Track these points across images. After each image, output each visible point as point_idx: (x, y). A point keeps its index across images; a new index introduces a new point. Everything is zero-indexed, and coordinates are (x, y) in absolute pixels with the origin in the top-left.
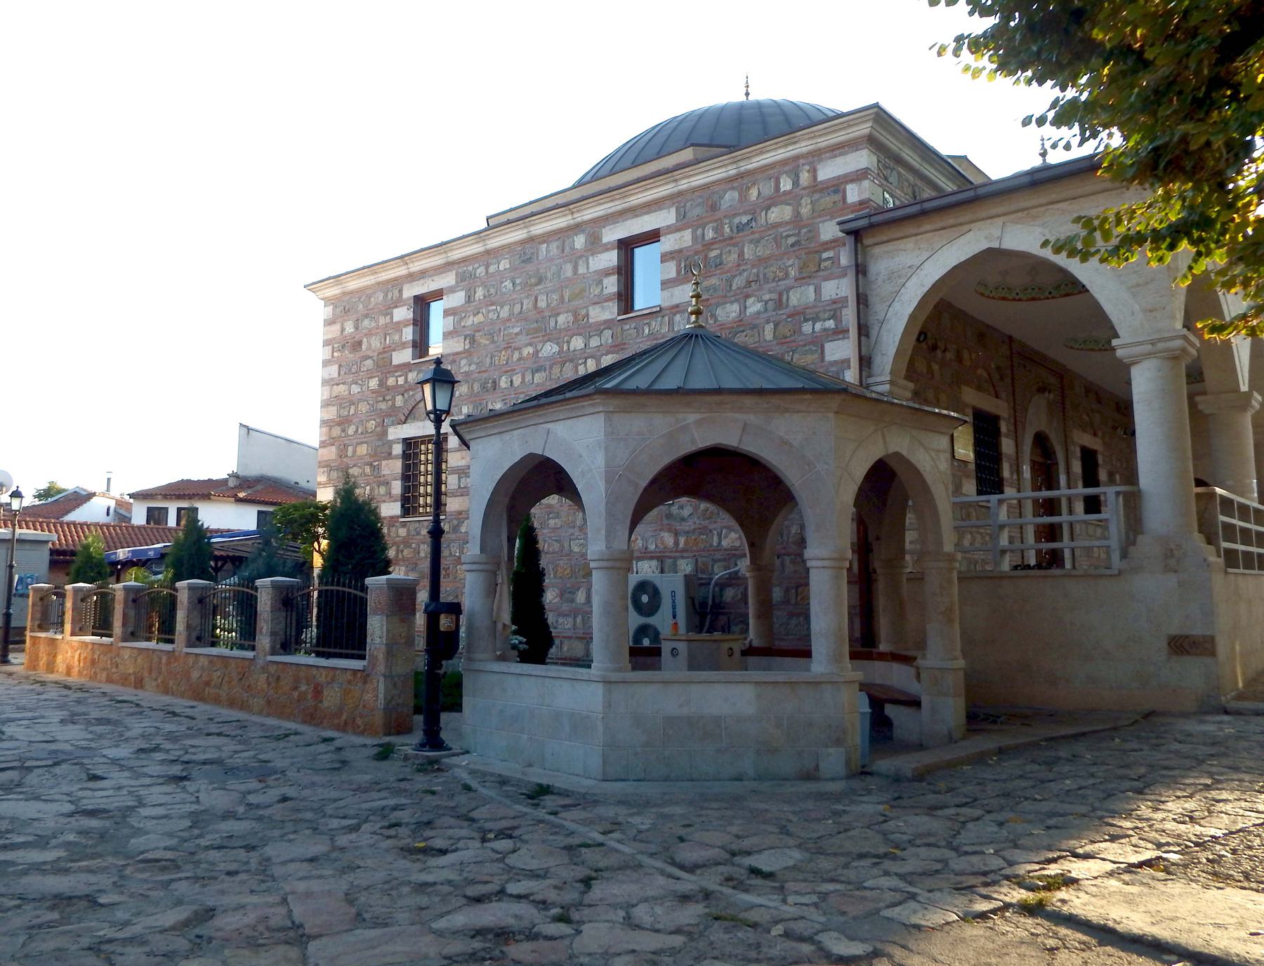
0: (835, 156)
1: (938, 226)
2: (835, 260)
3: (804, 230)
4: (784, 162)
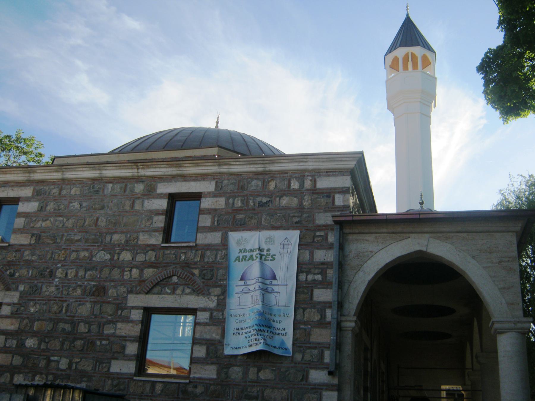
0: (329, 176)
2: (326, 238)
3: (305, 215)
4: (294, 172)
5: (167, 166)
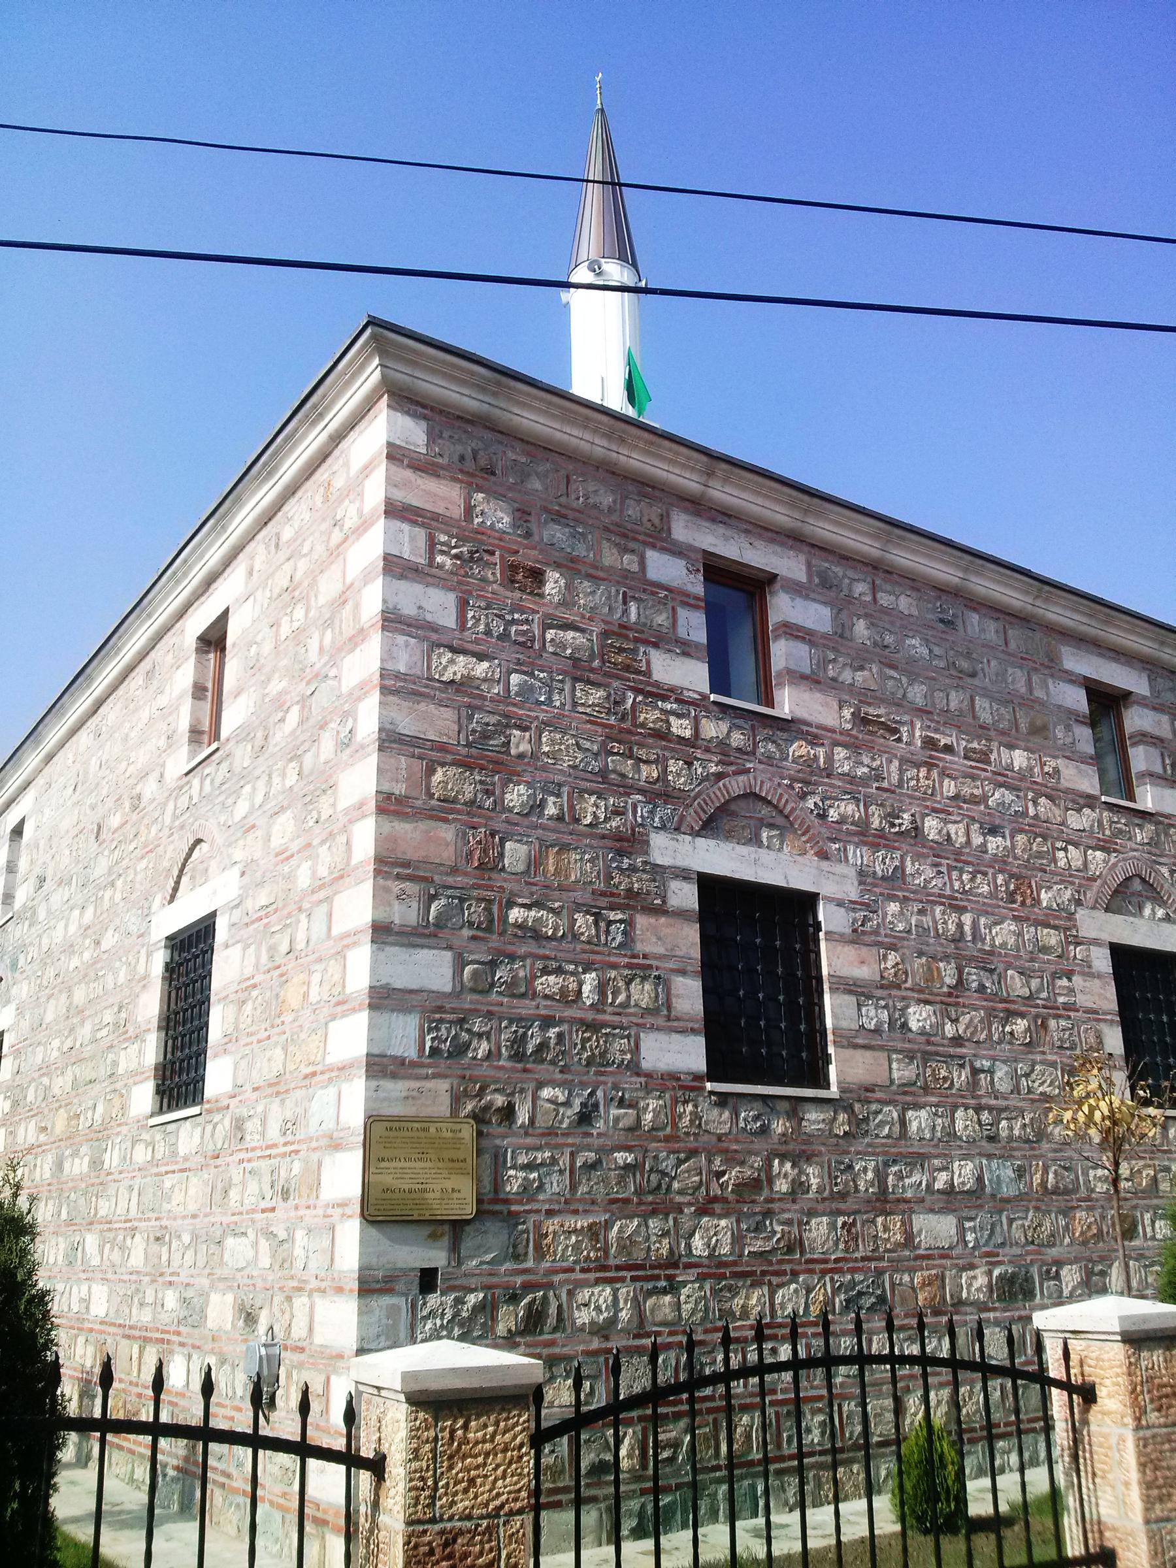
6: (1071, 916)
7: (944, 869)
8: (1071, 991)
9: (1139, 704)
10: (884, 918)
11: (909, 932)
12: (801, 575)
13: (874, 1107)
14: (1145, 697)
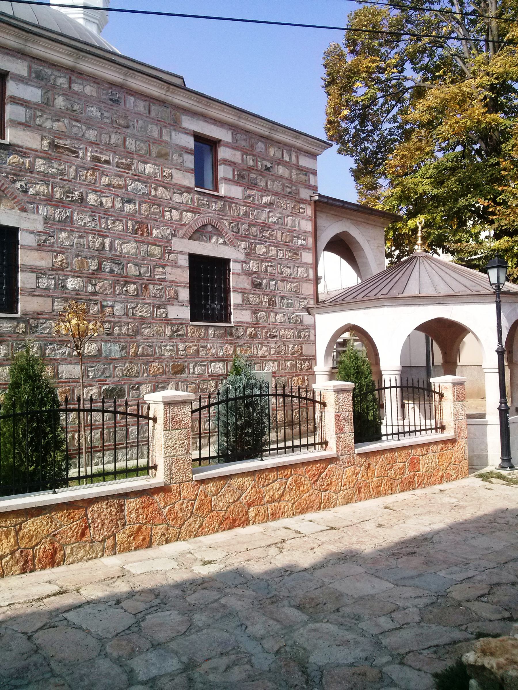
0: (305, 156)
1: (335, 214)
5: (197, 100)
6: (169, 241)
7: (97, 218)
8: (164, 273)
9: (224, 146)
10: (57, 240)
11: (72, 246)
12: (24, 72)
13: (41, 321)
14: (228, 143)
